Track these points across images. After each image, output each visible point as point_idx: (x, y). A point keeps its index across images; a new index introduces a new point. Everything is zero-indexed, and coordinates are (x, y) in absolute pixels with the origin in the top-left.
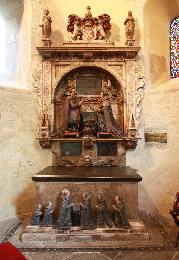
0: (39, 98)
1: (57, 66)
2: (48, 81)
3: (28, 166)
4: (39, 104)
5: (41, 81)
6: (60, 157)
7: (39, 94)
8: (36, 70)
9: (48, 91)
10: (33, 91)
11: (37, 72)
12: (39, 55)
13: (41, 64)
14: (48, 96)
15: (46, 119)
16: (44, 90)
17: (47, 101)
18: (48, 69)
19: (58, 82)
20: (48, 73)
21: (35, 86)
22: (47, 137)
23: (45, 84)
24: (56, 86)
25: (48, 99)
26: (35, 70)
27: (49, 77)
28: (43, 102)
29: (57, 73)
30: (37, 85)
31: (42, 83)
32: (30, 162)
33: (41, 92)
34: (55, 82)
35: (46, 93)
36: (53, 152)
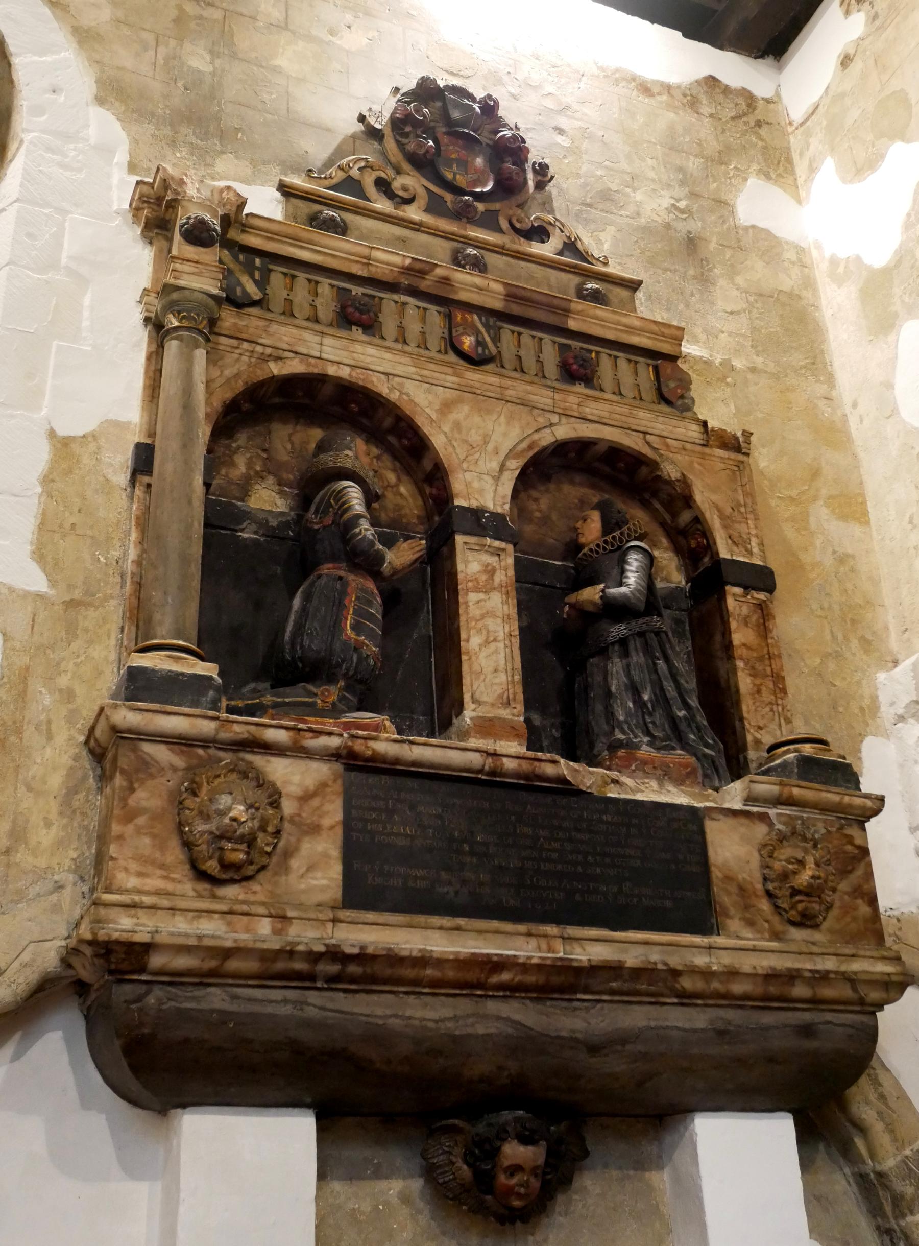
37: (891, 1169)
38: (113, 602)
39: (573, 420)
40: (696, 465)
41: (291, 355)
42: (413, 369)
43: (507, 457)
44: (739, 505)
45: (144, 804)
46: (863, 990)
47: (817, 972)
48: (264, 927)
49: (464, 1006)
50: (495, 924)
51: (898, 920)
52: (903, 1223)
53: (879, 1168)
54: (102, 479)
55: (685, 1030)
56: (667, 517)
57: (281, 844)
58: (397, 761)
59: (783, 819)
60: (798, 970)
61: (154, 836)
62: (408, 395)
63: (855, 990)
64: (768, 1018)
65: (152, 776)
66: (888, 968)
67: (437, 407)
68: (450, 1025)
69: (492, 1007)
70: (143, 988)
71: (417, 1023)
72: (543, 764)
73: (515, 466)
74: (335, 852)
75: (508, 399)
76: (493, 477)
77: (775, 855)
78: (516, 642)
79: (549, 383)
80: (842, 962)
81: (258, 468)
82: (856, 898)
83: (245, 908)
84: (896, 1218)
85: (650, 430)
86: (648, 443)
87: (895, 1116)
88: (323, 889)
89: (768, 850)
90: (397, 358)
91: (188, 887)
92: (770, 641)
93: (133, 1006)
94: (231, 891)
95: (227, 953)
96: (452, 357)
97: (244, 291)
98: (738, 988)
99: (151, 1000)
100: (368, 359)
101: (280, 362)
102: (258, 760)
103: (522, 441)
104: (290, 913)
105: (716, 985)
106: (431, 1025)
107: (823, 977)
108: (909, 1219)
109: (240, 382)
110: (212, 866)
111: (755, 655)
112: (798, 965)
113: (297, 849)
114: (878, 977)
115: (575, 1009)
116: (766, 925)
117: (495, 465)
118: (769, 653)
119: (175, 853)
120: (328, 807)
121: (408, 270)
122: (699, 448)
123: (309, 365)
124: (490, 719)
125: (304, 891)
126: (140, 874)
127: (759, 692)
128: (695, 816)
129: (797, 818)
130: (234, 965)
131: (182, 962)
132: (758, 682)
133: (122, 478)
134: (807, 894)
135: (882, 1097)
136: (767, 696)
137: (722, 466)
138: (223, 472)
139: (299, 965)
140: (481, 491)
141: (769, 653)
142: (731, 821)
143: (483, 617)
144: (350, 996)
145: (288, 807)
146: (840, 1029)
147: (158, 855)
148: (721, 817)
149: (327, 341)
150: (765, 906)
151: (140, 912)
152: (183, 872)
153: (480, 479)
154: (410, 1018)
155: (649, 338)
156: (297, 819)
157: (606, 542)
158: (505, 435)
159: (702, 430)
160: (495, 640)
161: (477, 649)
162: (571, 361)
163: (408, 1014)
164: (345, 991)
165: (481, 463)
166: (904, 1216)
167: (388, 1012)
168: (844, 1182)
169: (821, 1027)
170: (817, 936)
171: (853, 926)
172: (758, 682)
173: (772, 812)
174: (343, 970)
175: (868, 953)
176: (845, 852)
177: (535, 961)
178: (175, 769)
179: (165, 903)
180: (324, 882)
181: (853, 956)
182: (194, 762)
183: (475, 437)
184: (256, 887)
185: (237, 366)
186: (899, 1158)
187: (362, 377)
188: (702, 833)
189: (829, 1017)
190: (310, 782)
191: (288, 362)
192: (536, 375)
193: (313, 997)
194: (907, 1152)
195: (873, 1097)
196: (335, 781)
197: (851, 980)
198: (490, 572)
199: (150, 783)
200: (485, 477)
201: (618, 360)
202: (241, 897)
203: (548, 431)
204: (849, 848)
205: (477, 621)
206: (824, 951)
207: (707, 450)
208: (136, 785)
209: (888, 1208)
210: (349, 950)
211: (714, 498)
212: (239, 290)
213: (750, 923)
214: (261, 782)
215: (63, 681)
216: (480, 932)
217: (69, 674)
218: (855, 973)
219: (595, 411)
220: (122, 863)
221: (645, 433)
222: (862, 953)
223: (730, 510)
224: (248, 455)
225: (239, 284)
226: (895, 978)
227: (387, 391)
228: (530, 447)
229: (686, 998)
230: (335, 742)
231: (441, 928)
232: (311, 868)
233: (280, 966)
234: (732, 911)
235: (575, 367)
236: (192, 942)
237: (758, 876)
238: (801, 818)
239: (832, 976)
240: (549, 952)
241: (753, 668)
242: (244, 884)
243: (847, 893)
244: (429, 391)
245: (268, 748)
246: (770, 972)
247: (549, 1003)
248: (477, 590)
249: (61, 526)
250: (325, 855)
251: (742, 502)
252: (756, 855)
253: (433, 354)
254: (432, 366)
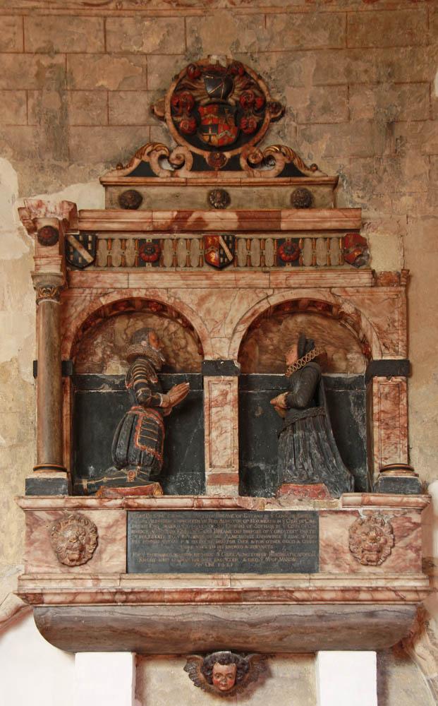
38: (32, 443)
39: (283, 290)
40: (367, 301)
41: (112, 290)
42: (182, 282)
43: (238, 324)
44: (394, 321)
45: (38, 537)
46: (402, 594)
47: (371, 587)
48: (89, 584)
49: (187, 609)
50: (198, 575)
54: (21, 381)
55: (301, 616)
56: (355, 333)
57: (98, 548)
58: (150, 507)
59: (366, 513)
60: (359, 587)
61: (42, 550)
62: (179, 298)
64: (348, 609)
65: (40, 525)
67: (196, 302)
68: (180, 618)
69: (201, 609)
70: (44, 610)
71: (165, 618)
72: (224, 500)
73: (243, 329)
74: (123, 550)
75: (240, 286)
76: (229, 339)
77: (357, 532)
78: (236, 432)
79: (268, 269)
80: (388, 582)
81: (108, 353)
82: (407, 550)
83: (81, 577)
85: (334, 285)
86: (333, 294)
88: (118, 565)
89: (353, 530)
90: (172, 277)
91: (58, 570)
92: (401, 406)
93: (42, 616)
94: (77, 570)
95: (76, 594)
96: (206, 268)
97: (84, 260)
98: (327, 596)
99: (49, 614)
100: (155, 282)
101: (106, 297)
102: (86, 513)
103: (247, 312)
104: (100, 577)
105: (314, 595)
106: (171, 618)
107: (376, 589)
109: (85, 314)
110: (67, 561)
111: (389, 416)
112: (360, 585)
113: (105, 550)
114: (409, 589)
115: (243, 609)
116: (348, 566)
117: (230, 331)
118: (399, 414)
119: (52, 557)
120: (119, 530)
121: (176, 219)
122: (369, 289)
123: (122, 294)
124: (219, 475)
125: (108, 568)
126: (38, 566)
127: (388, 438)
128: (314, 515)
129: (376, 511)
130: (79, 598)
131: (58, 599)
132: (389, 432)
133: (31, 379)
134: (368, 550)
136: (393, 439)
137: (385, 297)
138: (90, 359)
139: (107, 597)
140: (220, 349)
141: (399, 414)
142: (335, 517)
143: (219, 420)
144: (134, 608)
145: (101, 532)
146: (392, 613)
147: (45, 558)
148: (328, 515)
149: (132, 276)
150: (348, 557)
151: (36, 581)
152: (55, 563)
153: (220, 341)
154: (161, 616)
155: (337, 221)
156: (105, 537)
157: (299, 362)
158: (237, 310)
159: (371, 276)
160: (226, 432)
161: (215, 438)
162: (281, 252)
163: (161, 614)
164: (132, 606)
165: (221, 331)
167: (152, 614)
169: (380, 612)
170: (378, 570)
171: (402, 564)
172: (389, 432)
173: (360, 510)
174: (127, 598)
175: (405, 577)
176: (404, 527)
177: (214, 590)
178: (50, 521)
179: (47, 577)
180: (118, 563)
182: (58, 517)
183: (218, 316)
184: (86, 567)
185: (84, 304)
187: (152, 294)
188: (317, 524)
189: (385, 607)
190: (111, 521)
191: (111, 295)
192: (260, 266)
193: (118, 609)
196: (122, 519)
198: (225, 394)
199: (39, 528)
200: (224, 339)
201: (317, 241)
202: (81, 572)
203: (265, 301)
204: (407, 524)
205: (216, 423)
206: (378, 577)
207: (375, 289)
208: (33, 530)
210: (126, 590)
211: (376, 320)
212: (80, 259)
213: (339, 566)
214: (87, 521)
215: (13, 483)
216: (189, 579)
217: (15, 480)
218: (395, 587)
219: (297, 281)
220: (30, 562)
221: (331, 288)
223: (387, 326)
224: (103, 347)
225: (80, 255)
226: (418, 589)
227: (167, 299)
228: (253, 315)
229: (300, 602)
230: (119, 502)
231: (170, 579)
232: (111, 558)
233: (100, 597)
234: (328, 561)
235: (283, 256)
236: (59, 591)
237: (346, 543)
238: (379, 511)
239: (380, 589)
240: (223, 585)
241: (387, 424)
242: (82, 566)
243: (402, 548)
244: (191, 293)
245: (89, 508)
246: (342, 588)
247: (229, 607)
248: (217, 406)
249: (5, 410)
250: (118, 552)
251: (397, 319)
252: (347, 533)
253: (195, 269)
254: (193, 277)
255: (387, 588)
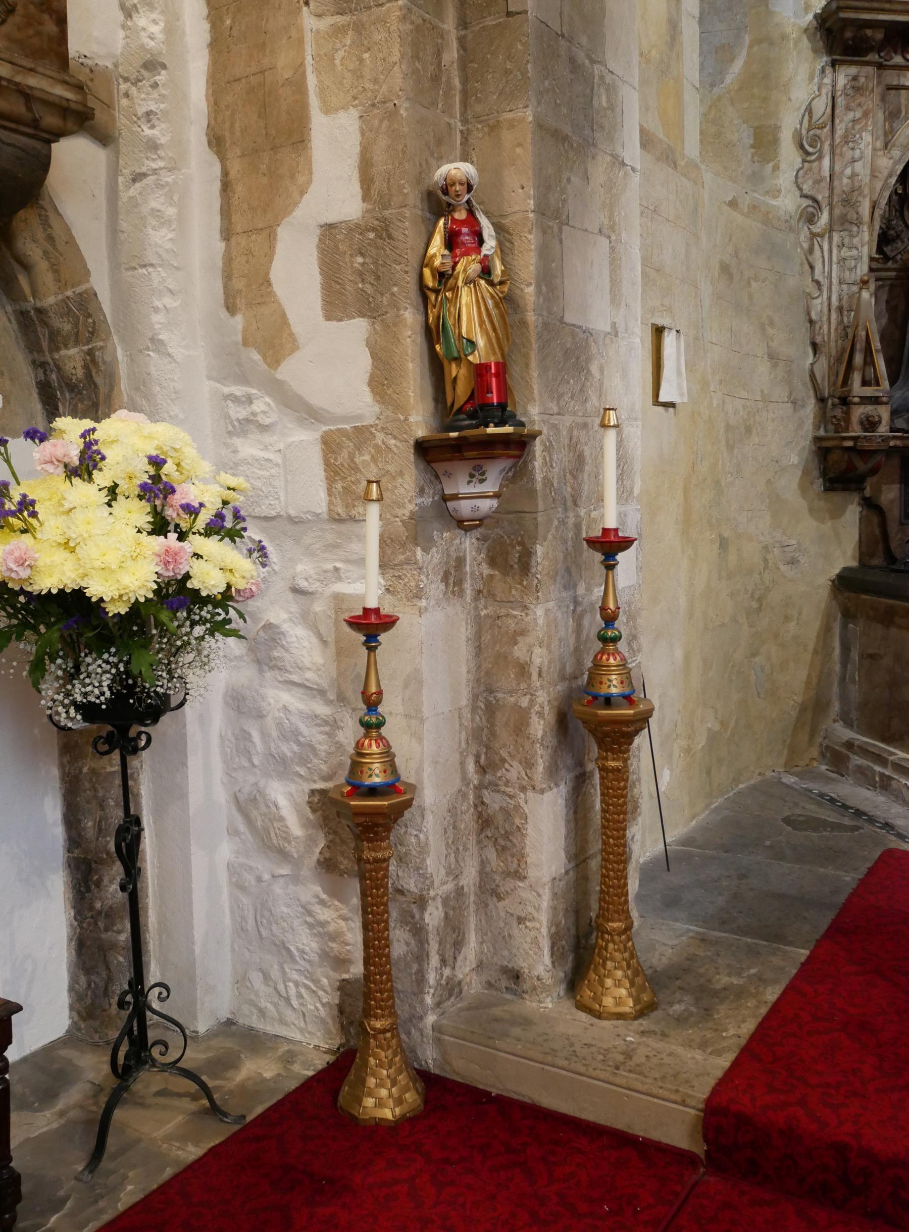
0: (816, 247)
1: (894, 92)
2: (858, 166)
3: (783, 568)
4: (816, 277)
5: (826, 162)
6: (902, 524)
7: (816, 229)
8: (809, 110)
9: (855, 216)
10: (797, 210)
11: (810, 117)
12: (815, 34)
13: (827, 80)
14: (856, 241)
15: (877, 351)
16: (837, 212)
17: (853, 263)
18: (859, 105)
19: (899, 172)
20: (857, 127)
21: (800, 189)
22: (883, 429)
23: (845, 181)
24: (887, 194)
25: (854, 252)
26: (804, 107)
27: (862, 146)
28: (834, 266)
29: (891, 127)
30: (810, 182)
31: (827, 174)
32: (787, 548)
33: (824, 218)
34: (886, 173)
35: (847, 225)
36: (870, 505)
37: (51, 306)
46: (39, 110)
51: (92, 71)
52: (56, 356)
53: (39, 304)
63: (29, 109)
66: (69, 95)
80: (18, 73)
84: (51, 352)
87: (61, 258)
108: (63, 352)
114: (57, 101)
135: (50, 239)
146: (9, 149)
166: (58, 349)
168: (5, 319)
175: (48, 72)
181: (31, 70)
186: (60, 297)
194: (69, 293)
195: (40, 235)
197: (26, 95)
209: (45, 345)
218: (31, 88)
222: (40, 69)
226: (73, 106)
255: (17, 84)
